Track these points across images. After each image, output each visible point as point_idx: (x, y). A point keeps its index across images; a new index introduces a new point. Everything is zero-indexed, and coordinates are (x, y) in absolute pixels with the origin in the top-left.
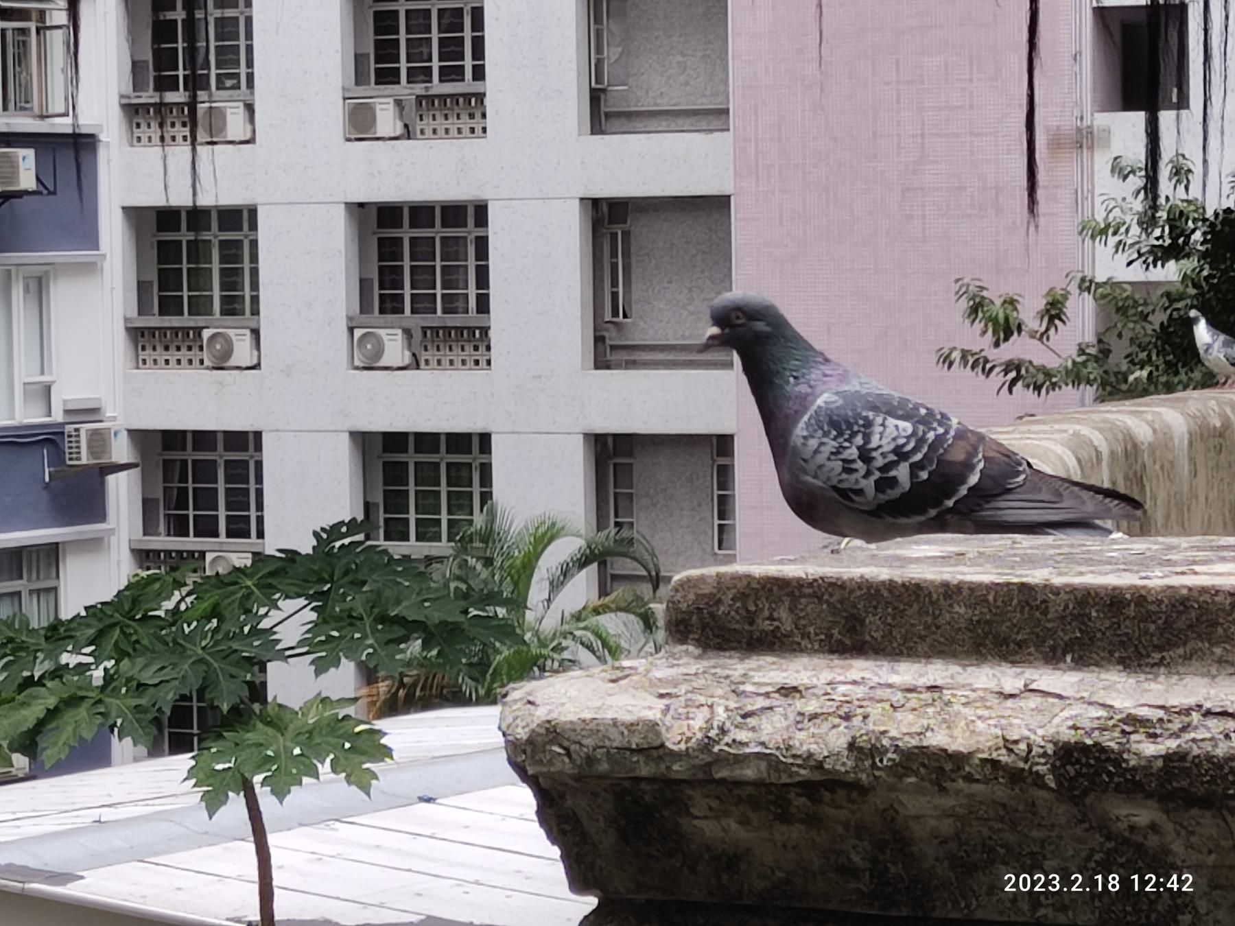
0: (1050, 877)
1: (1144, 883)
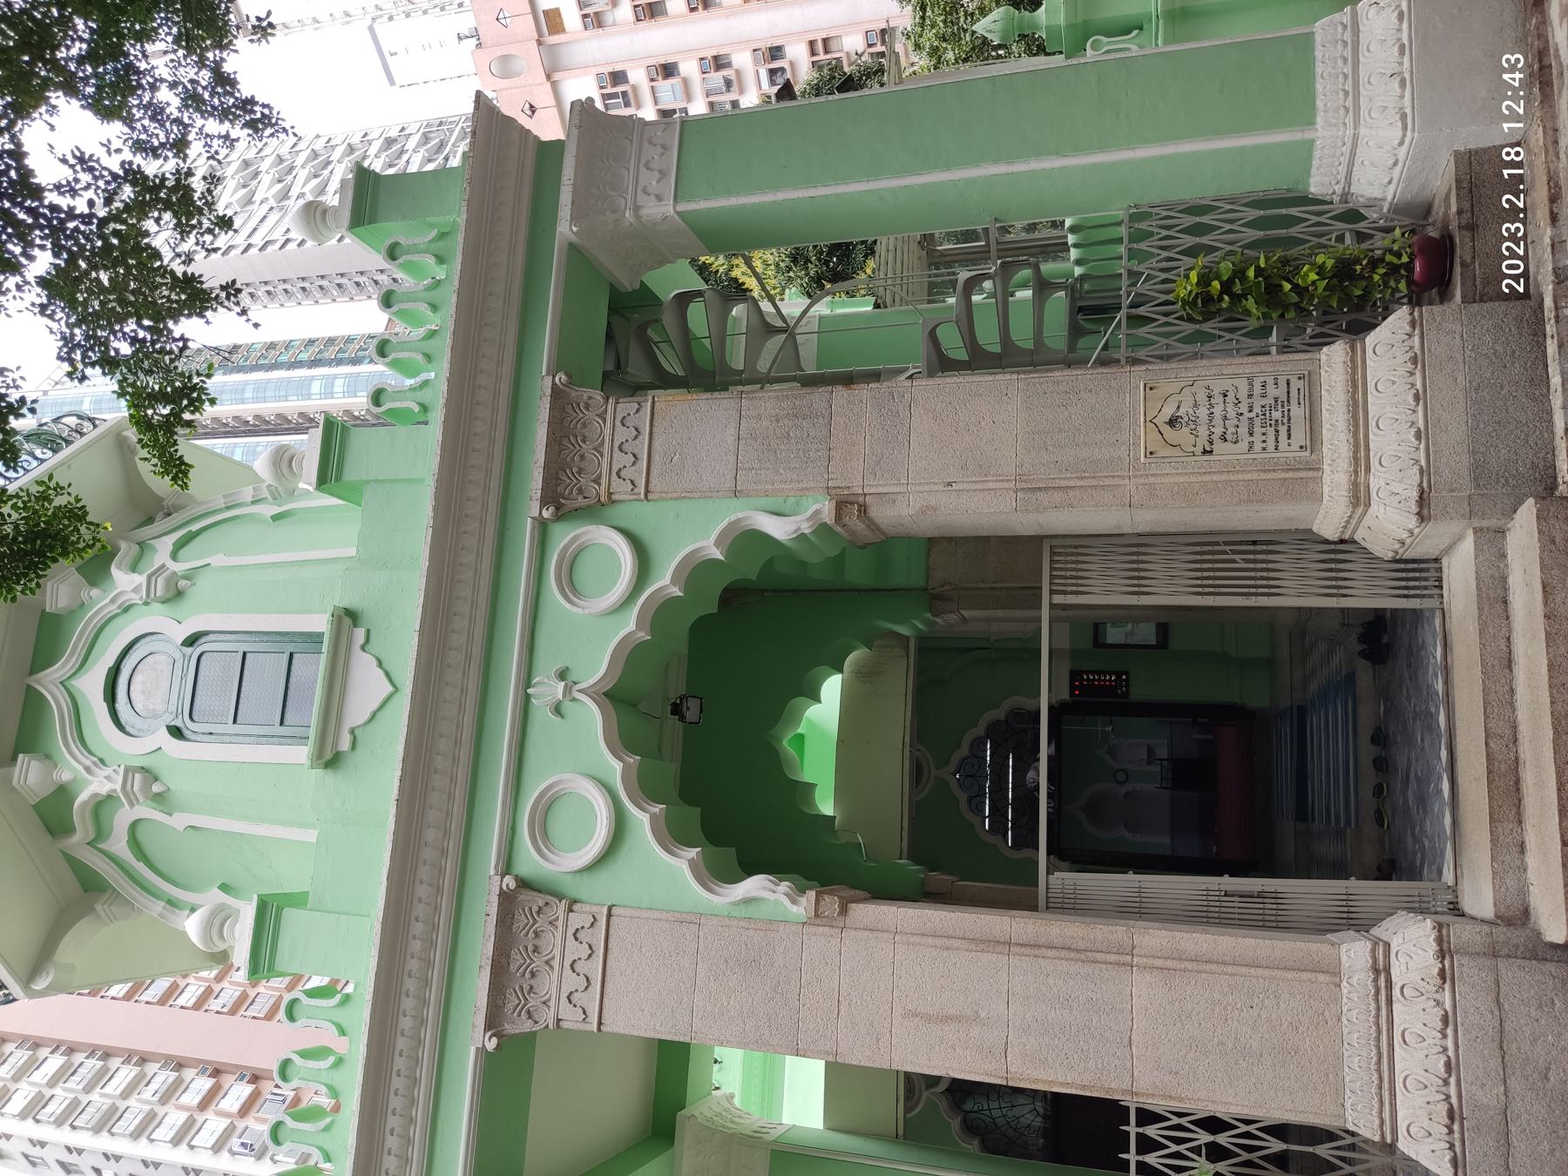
0: (1506, 234)
1: (1514, 117)
